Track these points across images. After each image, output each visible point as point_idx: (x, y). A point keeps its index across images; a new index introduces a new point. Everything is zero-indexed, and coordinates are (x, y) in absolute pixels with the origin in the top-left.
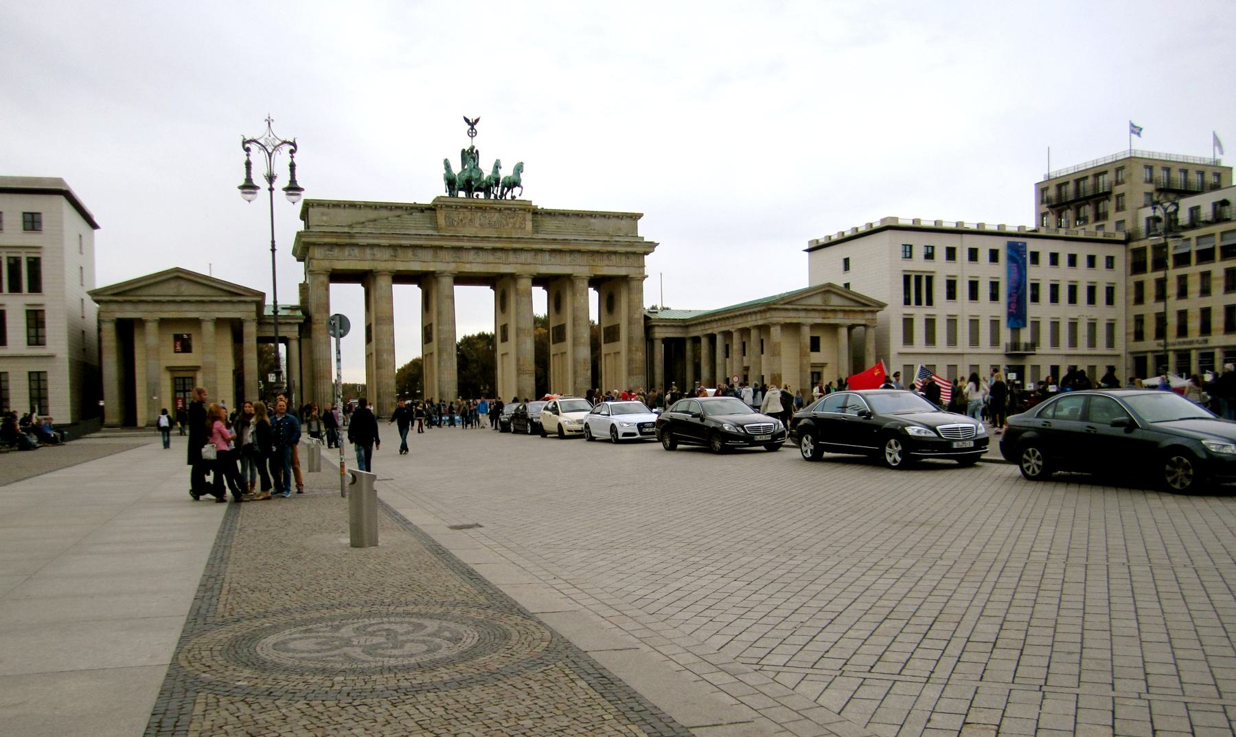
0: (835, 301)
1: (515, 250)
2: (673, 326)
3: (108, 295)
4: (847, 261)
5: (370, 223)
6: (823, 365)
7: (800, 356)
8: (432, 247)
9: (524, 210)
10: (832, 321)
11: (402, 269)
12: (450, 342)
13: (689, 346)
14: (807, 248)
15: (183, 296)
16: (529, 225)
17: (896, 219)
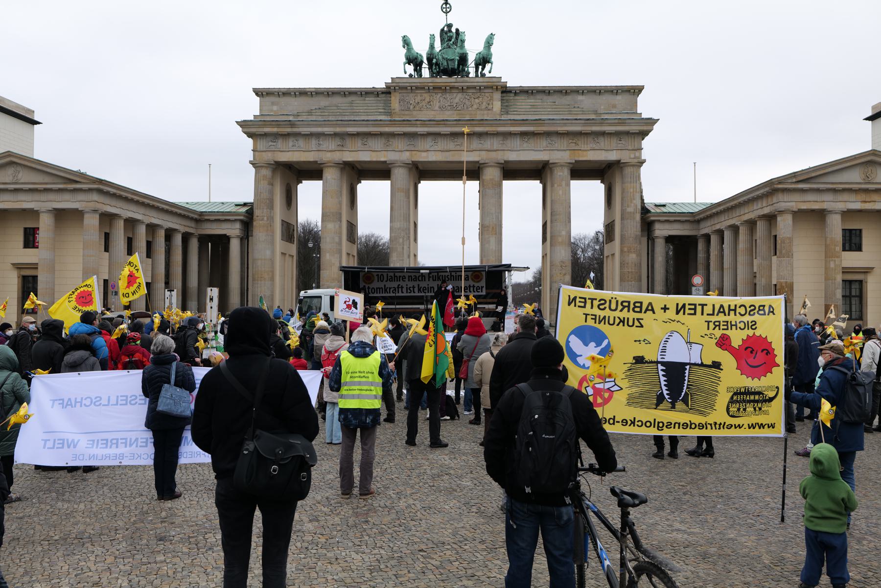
1: (480, 135)
2: (679, 221)
6: (867, 271)
8: (381, 134)
9: (492, 87)
12: (401, 240)
13: (701, 246)
14: (869, 114)
16: (497, 105)
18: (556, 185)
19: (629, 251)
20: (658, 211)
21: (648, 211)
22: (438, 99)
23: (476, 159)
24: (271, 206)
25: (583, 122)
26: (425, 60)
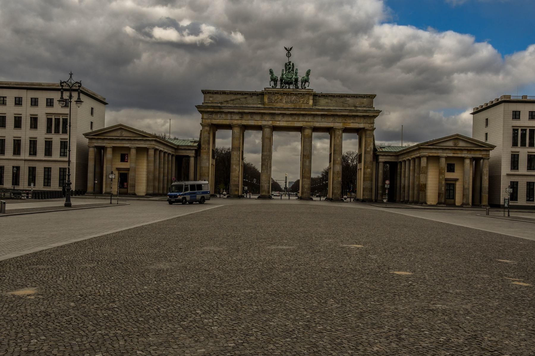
0: (461, 144)
1: (303, 115)
3: (91, 136)
4: (487, 119)
5: (231, 101)
6: (456, 180)
7: (439, 174)
8: (260, 113)
9: (309, 94)
10: (459, 155)
11: (245, 124)
12: (267, 160)
13: (399, 167)
14: (472, 112)
15: (123, 137)
16: (311, 102)
17: (509, 97)
18: (336, 138)
19: (367, 168)
20: (381, 150)
21: (376, 150)
22: (285, 99)
23: (301, 125)
24: (209, 144)
25: (349, 111)
26: (279, 79)
